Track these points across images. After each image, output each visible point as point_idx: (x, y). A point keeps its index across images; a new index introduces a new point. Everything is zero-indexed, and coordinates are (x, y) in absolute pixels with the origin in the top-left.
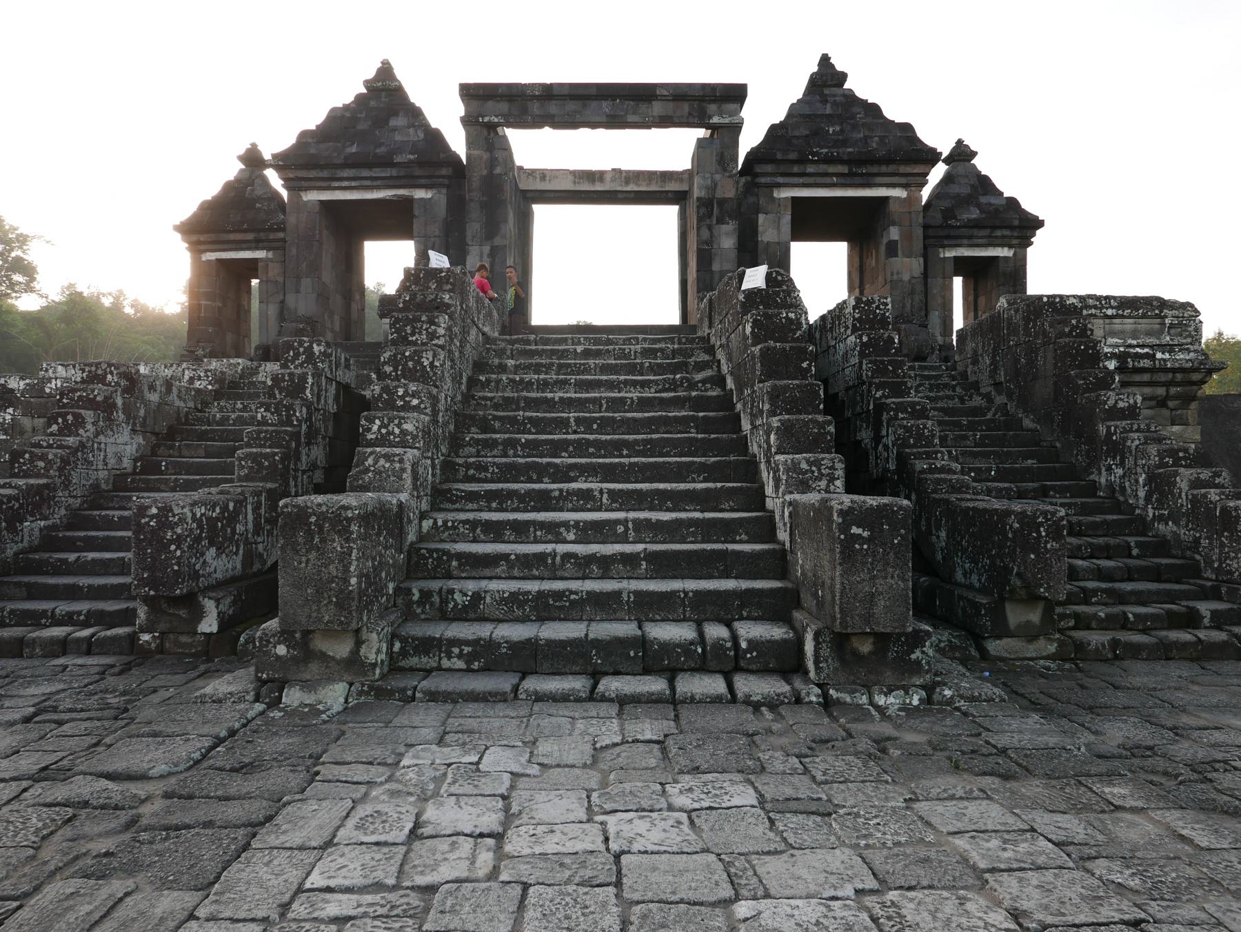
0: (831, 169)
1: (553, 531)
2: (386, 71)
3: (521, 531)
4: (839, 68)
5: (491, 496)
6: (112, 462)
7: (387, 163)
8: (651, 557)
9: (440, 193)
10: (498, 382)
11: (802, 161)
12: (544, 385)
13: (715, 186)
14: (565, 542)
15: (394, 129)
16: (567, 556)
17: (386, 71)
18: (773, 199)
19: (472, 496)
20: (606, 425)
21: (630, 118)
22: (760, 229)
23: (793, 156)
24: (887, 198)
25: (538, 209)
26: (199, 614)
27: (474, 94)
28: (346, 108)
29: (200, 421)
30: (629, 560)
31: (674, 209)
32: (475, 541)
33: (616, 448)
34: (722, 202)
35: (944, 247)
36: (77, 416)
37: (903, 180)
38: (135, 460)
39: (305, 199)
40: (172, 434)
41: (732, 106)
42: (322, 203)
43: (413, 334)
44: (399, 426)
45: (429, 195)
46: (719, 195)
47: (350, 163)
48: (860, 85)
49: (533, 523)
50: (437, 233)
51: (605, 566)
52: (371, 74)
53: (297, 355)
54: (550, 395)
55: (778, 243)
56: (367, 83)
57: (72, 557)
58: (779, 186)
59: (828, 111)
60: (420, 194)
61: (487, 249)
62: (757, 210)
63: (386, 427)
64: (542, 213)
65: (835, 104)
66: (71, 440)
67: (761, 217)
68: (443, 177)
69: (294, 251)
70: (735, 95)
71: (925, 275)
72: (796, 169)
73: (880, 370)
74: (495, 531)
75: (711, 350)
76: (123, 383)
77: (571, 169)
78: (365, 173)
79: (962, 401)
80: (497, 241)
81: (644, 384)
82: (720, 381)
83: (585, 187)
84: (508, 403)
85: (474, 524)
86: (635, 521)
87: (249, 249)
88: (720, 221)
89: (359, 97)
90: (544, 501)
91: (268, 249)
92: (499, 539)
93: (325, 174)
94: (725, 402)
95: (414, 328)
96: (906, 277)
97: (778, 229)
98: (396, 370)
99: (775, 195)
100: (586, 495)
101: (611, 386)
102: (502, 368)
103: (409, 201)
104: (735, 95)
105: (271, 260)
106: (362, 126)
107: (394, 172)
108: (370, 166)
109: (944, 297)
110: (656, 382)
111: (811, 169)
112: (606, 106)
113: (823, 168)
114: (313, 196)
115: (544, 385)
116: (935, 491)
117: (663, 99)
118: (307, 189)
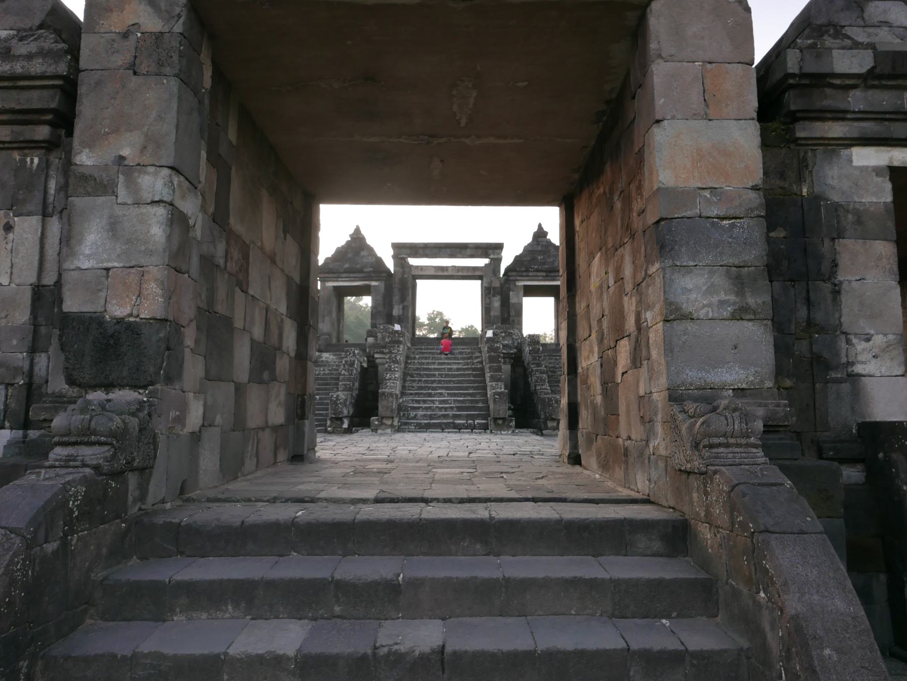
0: (539, 274)
1: (433, 402)
2: (357, 230)
3: (425, 402)
4: (545, 229)
5: (416, 394)
7: (361, 271)
8: (457, 407)
11: (527, 271)
12: (428, 364)
13: (492, 282)
15: (363, 257)
17: (357, 230)
18: (516, 286)
19: (411, 394)
20: (447, 376)
23: (523, 269)
25: (418, 281)
26: (343, 423)
27: (396, 246)
28: (343, 247)
33: (450, 382)
34: (494, 288)
41: (498, 251)
46: (493, 285)
47: (346, 271)
52: (352, 232)
56: (351, 236)
59: (539, 248)
60: (374, 283)
61: (401, 307)
62: (509, 290)
64: (422, 285)
65: (542, 246)
67: (511, 293)
70: (499, 247)
72: (525, 274)
73: (534, 359)
74: (418, 402)
75: (480, 352)
78: (352, 275)
80: (405, 304)
81: (459, 363)
82: (481, 362)
83: (440, 273)
84: (418, 369)
88: (494, 296)
89: (348, 242)
90: (430, 395)
93: (336, 275)
94: (482, 369)
100: (441, 394)
101: (448, 364)
102: (415, 358)
104: (499, 247)
106: (350, 255)
107: (363, 275)
108: (354, 272)
111: (531, 274)
112: (448, 251)
113: (535, 273)
114: (330, 284)
115: (428, 364)
117: (471, 248)
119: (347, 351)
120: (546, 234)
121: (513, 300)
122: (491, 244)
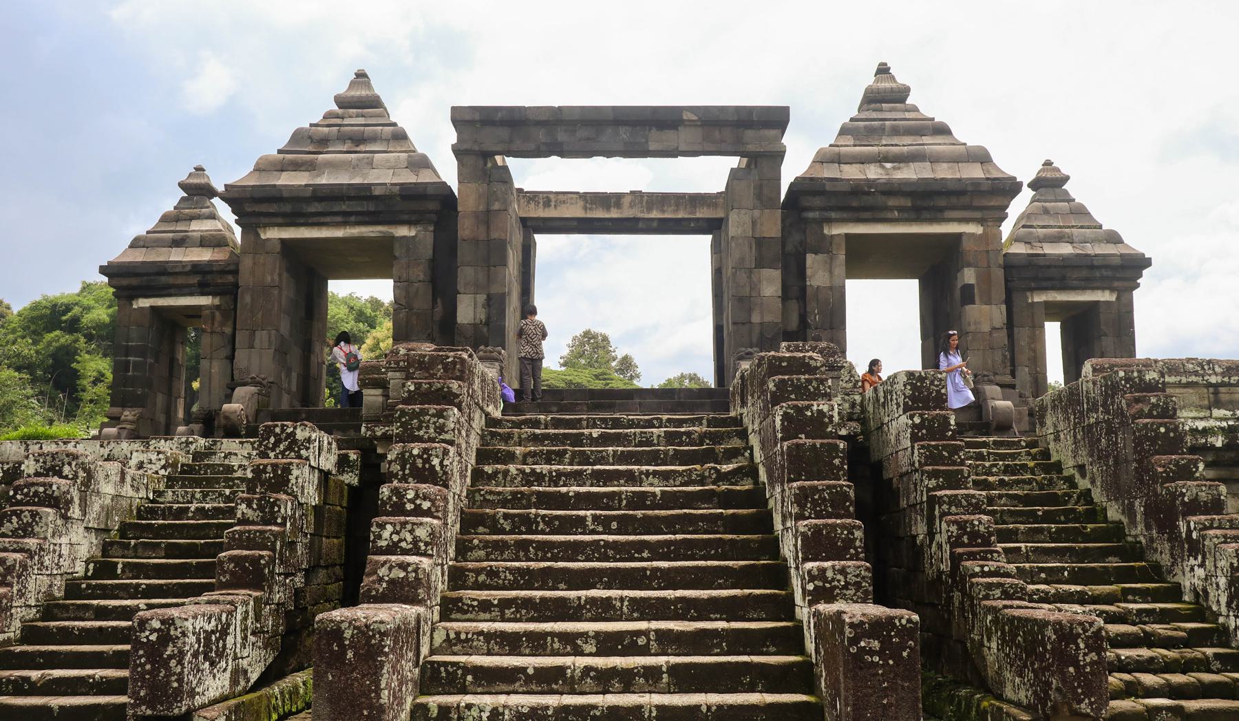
3: (537, 643)
5: (505, 603)
6: (65, 563)
8: (673, 669)
9: (426, 230)
10: (506, 472)
12: (555, 479)
14: (582, 654)
16: (587, 670)
19: (485, 606)
20: (626, 525)
21: (653, 146)
22: (809, 272)
24: (959, 236)
27: (465, 119)
29: (152, 513)
30: (652, 674)
31: (706, 240)
32: (489, 653)
35: (1032, 290)
36: (34, 515)
37: (978, 215)
38: (87, 562)
39: (263, 237)
40: (124, 529)
41: (773, 133)
42: (283, 241)
43: (419, 429)
44: (412, 532)
45: (413, 233)
48: (927, 102)
49: (553, 634)
50: (422, 277)
51: (627, 680)
53: (276, 444)
54: (564, 490)
55: (831, 288)
57: (35, 675)
58: (830, 221)
60: (403, 231)
61: (482, 298)
63: (398, 533)
66: (32, 543)
67: (810, 258)
68: (431, 212)
69: (248, 299)
70: (776, 119)
71: (1010, 324)
73: (932, 457)
74: (512, 643)
75: (743, 435)
76: (82, 474)
77: (581, 191)
79: (1041, 487)
81: (665, 476)
82: (752, 471)
83: (600, 214)
84: (516, 499)
85: (488, 636)
86: (657, 631)
87: (191, 294)
91: (214, 294)
92: (515, 651)
94: (757, 498)
95: (421, 422)
96: (986, 328)
97: (831, 272)
98: (403, 469)
99: (826, 232)
101: (631, 478)
102: (510, 457)
103: (392, 239)
104: (776, 119)
105: (218, 307)
109: (1034, 351)
110: (680, 474)
112: (624, 133)
114: (273, 234)
116: (986, 597)
118: (266, 226)
119: (269, 431)
120: (899, 95)
121: (817, 273)
122: (750, 110)
